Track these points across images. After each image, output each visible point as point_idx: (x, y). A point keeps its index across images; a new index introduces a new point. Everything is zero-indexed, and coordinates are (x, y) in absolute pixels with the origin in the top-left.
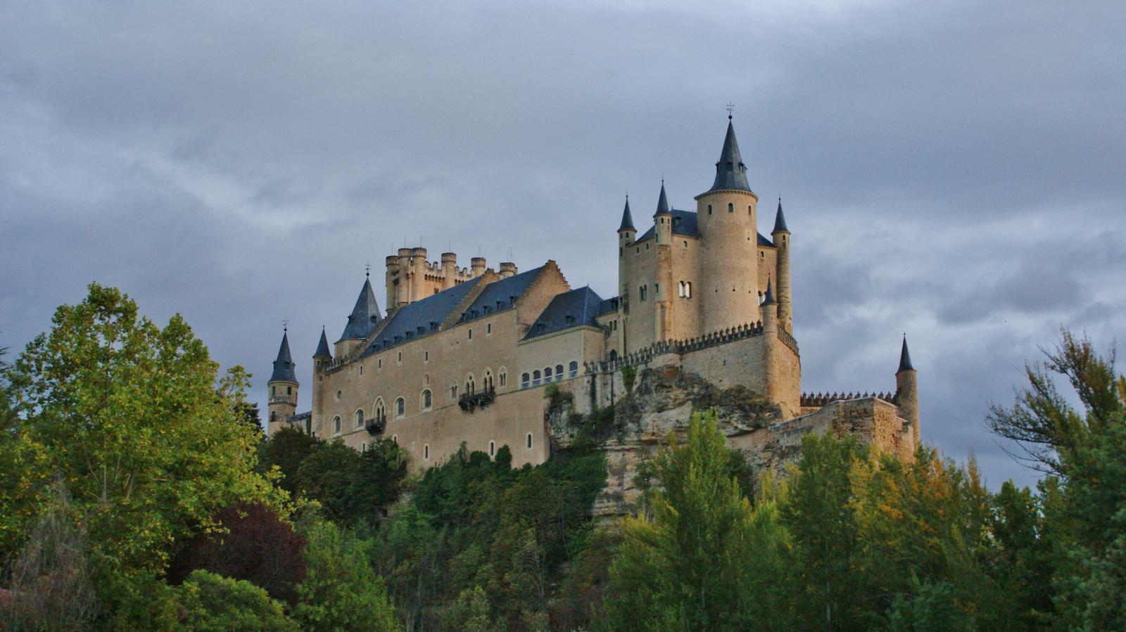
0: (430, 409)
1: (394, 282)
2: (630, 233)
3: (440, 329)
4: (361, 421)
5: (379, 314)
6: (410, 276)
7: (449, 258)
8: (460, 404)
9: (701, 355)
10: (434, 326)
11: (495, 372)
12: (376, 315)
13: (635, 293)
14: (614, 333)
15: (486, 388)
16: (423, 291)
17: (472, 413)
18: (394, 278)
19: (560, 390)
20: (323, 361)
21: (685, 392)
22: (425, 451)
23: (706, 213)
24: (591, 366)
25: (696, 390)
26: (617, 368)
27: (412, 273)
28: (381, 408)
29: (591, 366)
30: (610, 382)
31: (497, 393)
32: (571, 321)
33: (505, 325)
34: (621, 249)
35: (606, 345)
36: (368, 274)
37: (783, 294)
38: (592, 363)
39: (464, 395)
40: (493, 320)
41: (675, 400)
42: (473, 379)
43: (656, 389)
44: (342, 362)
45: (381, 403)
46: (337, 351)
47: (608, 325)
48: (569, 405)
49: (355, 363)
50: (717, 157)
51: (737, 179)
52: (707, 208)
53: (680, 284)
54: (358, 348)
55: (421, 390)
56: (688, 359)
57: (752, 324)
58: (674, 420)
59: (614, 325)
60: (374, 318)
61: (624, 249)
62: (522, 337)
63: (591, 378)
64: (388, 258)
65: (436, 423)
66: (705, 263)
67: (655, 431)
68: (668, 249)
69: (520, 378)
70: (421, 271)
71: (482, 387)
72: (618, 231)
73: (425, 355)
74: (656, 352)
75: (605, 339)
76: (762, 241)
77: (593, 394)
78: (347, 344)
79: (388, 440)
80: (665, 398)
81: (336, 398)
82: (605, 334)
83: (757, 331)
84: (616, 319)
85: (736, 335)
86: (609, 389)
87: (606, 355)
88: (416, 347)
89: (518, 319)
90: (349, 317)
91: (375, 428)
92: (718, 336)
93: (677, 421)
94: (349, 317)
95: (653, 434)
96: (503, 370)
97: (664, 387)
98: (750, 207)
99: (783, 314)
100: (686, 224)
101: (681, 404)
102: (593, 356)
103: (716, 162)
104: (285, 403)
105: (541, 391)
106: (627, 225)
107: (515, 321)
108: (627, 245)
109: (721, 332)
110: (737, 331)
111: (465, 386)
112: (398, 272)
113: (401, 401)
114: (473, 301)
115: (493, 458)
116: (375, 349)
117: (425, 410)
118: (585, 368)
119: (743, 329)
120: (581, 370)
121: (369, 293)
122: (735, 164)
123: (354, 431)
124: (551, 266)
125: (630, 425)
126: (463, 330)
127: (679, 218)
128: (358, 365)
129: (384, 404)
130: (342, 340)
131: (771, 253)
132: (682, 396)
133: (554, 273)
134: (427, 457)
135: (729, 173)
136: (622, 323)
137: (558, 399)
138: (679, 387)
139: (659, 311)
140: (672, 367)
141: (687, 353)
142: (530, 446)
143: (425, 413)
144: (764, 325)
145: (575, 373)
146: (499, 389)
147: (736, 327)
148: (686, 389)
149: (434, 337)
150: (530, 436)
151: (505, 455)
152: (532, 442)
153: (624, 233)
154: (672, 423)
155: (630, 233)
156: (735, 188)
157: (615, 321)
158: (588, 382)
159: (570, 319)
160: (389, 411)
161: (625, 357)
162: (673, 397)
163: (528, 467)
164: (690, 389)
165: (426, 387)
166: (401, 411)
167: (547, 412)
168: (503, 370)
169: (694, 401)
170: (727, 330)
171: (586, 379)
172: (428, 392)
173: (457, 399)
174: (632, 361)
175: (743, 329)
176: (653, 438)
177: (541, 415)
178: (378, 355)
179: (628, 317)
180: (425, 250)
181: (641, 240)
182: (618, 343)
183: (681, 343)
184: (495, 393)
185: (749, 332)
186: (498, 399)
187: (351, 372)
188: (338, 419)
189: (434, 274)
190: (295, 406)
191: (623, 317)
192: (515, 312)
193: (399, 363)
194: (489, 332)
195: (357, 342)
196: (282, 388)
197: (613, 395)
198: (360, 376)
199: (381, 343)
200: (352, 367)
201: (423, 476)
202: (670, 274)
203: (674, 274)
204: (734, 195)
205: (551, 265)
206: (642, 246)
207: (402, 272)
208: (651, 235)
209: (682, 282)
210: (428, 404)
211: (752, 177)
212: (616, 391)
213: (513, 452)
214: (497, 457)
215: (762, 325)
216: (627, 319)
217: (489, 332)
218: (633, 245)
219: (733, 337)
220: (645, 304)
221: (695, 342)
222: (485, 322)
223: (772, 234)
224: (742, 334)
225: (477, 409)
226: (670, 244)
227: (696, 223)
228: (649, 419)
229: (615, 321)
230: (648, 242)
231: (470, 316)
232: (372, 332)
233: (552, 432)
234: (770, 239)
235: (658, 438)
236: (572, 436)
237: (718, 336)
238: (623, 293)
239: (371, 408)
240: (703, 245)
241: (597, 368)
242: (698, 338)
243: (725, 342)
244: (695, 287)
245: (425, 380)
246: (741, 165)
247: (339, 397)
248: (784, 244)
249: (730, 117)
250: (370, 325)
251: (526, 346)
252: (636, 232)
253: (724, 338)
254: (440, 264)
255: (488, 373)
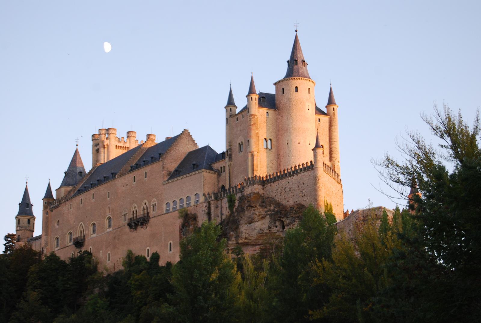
0: (111, 229)
1: (97, 152)
2: (233, 108)
3: (117, 176)
4: (70, 240)
5: (84, 170)
6: (106, 146)
7: (131, 134)
8: (128, 225)
9: (275, 185)
10: (114, 175)
11: (149, 202)
12: (82, 172)
13: (236, 147)
14: (223, 174)
15: (144, 214)
16: (115, 153)
17: (136, 230)
18: (96, 148)
19: (189, 212)
20: (48, 202)
21: (265, 210)
22: (108, 257)
23: (281, 93)
24: (208, 196)
25: (272, 208)
26: (224, 196)
27: (107, 145)
28: (82, 230)
29: (208, 196)
30: (220, 206)
31: (150, 217)
32: (196, 167)
33: (155, 172)
34: (227, 119)
35: (218, 182)
36: (77, 145)
37: (333, 146)
38: (209, 194)
39: (131, 219)
40: (148, 169)
41: (259, 215)
42: (136, 208)
43: (247, 209)
44: (60, 201)
45: (83, 227)
46: (57, 195)
47: (220, 169)
48: (194, 222)
49: (67, 202)
50: (288, 58)
51: (301, 71)
52: (281, 90)
53: (264, 140)
54: (70, 192)
55: (105, 217)
56: (267, 188)
57: (307, 163)
58: (258, 228)
59: (223, 169)
60: (81, 173)
61: (229, 119)
62: (166, 179)
63: (207, 204)
64: (93, 136)
65: (115, 238)
66: (280, 126)
67: (247, 236)
68: (256, 117)
69: (164, 206)
70: (113, 143)
71: (142, 213)
72: (225, 107)
73: (108, 193)
74: (247, 184)
75: (218, 178)
76: (319, 111)
77: (209, 214)
78: (63, 189)
79: (86, 252)
80: (253, 214)
81: (56, 225)
82: (218, 176)
83: (310, 167)
84: (224, 165)
85: (297, 171)
86: (219, 211)
87: (218, 189)
88: (102, 189)
89: (163, 167)
90: (65, 173)
91: (79, 243)
92: (286, 172)
93: (261, 229)
94: (65, 173)
95: (246, 238)
96: (154, 201)
97: (252, 207)
98: (309, 89)
99: (334, 159)
100: (268, 101)
101: (263, 218)
102: (209, 189)
103: (287, 60)
104: (26, 229)
105: (177, 214)
106: (231, 102)
107: (161, 169)
108: (230, 116)
109: (288, 169)
110: (297, 168)
111: (132, 213)
112: (98, 144)
113: (94, 224)
114: (138, 158)
115: (148, 259)
116: (80, 192)
117: (108, 230)
118: (204, 197)
119: (301, 167)
120: (202, 199)
121: (78, 157)
122: (299, 61)
123: (67, 246)
124: (185, 133)
125: (232, 233)
126: (129, 178)
127: (263, 97)
128: (68, 203)
129: (84, 227)
130: (60, 187)
131: (325, 119)
132: (263, 213)
133: (187, 137)
134: (109, 260)
135: (295, 67)
136: (228, 167)
138: (262, 206)
139: (250, 158)
140: (258, 193)
141: (266, 184)
142: (171, 250)
143: (108, 232)
144: (314, 163)
145: (198, 201)
146: (152, 214)
147: (297, 165)
148: (266, 208)
149: (113, 183)
150: (171, 244)
151: (156, 257)
152: (172, 248)
153: (229, 108)
154: (256, 231)
155: (233, 108)
156: (299, 76)
157: (224, 166)
158: (206, 206)
159: (195, 166)
160: (87, 232)
161: (229, 189)
162: (258, 213)
163: (169, 264)
164: (268, 207)
165: (109, 215)
166: (94, 231)
167: (181, 227)
168: (154, 201)
169: (271, 216)
170: (291, 168)
171: (205, 205)
172: (110, 218)
173: (127, 222)
174: (233, 191)
175: (301, 167)
176: (246, 241)
177: (177, 229)
178: (80, 196)
179: (232, 163)
180: (115, 130)
181: (239, 113)
182: (225, 180)
183: (263, 178)
184: (149, 216)
185: (305, 168)
186: (152, 221)
187: (64, 208)
188: (57, 238)
189: (121, 145)
190: (33, 231)
191: (228, 163)
192: (161, 163)
193: (93, 200)
194: (146, 177)
195: (69, 189)
196: (24, 220)
197: (222, 214)
198: (70, 210)
199: (83, 189)
200: (66, 204)
201: (106, 275)
202: (257, 133)
203: (260, 134)
204: (299, 80)
205: (185, 133)
206: (241, 115)
207: (101, 144)
208: (246, 109)
209: (265, 139)
210: (110, 226)
211: (311, 69)
213: (161, 255)
214: (151, 258)
215: (313, 163)
216: (231, 164)
217: (146, 177)
218: (234, 116)
219: (296, 172)
220: (242, 154)
221: (272, 177)
222: (143, 171)
223: (326, 107)
224: (301, 170)
225: (139, 228)
226: (257, 113)
227: (275, 101)
228: (243, 228)
229: (224, 166)
230: (243, 114)
231: (137, 166)
232: (78, 181)
234: (325, 110)
235: (249, 241)
237: (286, 172)
238: (228, 148)
239: (77, 230)
240: (279, 114)
241: (211, 197)
242: (273, 174)
243: (290, 176)
244: (274, 142)
245: (108, 211)
246: (303, 61)
247: (58, 225)
248: (334, 114)
249: (296, 31)
250: (78, 177)
251: (168, 185)
252: (237, 107)
253: (289, 173)
254: (125, 138)
255: (146, 204)
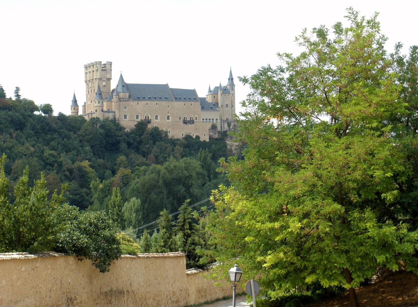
0: (169, 121)
11: (194, 116)
28: (147, 116)
96: (196, 116)
117: (168, 121)
137: (214, 127)
146: (195, 121)
151: (198, 137)
173: (182, 120)
186: (195, 123)
212: (225, 127)
233: (211, 134)
236: (218, 136)
